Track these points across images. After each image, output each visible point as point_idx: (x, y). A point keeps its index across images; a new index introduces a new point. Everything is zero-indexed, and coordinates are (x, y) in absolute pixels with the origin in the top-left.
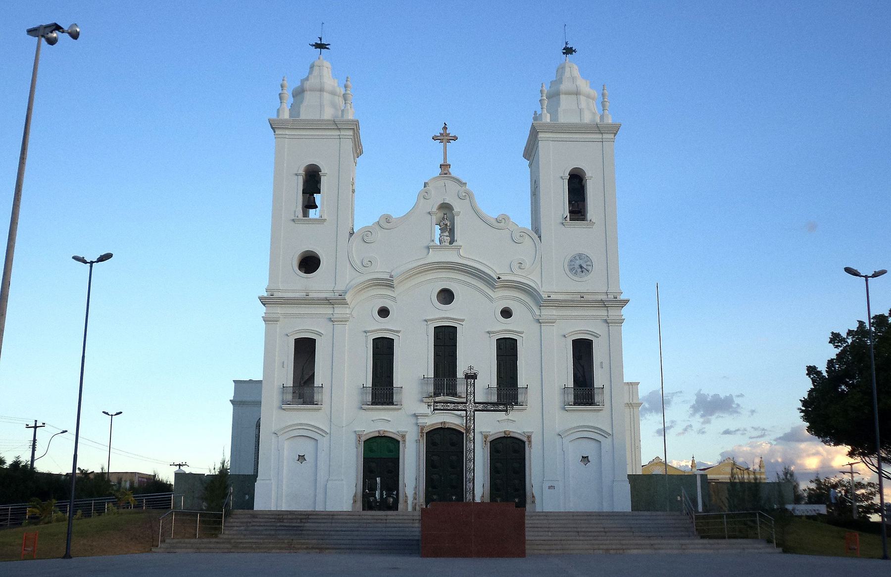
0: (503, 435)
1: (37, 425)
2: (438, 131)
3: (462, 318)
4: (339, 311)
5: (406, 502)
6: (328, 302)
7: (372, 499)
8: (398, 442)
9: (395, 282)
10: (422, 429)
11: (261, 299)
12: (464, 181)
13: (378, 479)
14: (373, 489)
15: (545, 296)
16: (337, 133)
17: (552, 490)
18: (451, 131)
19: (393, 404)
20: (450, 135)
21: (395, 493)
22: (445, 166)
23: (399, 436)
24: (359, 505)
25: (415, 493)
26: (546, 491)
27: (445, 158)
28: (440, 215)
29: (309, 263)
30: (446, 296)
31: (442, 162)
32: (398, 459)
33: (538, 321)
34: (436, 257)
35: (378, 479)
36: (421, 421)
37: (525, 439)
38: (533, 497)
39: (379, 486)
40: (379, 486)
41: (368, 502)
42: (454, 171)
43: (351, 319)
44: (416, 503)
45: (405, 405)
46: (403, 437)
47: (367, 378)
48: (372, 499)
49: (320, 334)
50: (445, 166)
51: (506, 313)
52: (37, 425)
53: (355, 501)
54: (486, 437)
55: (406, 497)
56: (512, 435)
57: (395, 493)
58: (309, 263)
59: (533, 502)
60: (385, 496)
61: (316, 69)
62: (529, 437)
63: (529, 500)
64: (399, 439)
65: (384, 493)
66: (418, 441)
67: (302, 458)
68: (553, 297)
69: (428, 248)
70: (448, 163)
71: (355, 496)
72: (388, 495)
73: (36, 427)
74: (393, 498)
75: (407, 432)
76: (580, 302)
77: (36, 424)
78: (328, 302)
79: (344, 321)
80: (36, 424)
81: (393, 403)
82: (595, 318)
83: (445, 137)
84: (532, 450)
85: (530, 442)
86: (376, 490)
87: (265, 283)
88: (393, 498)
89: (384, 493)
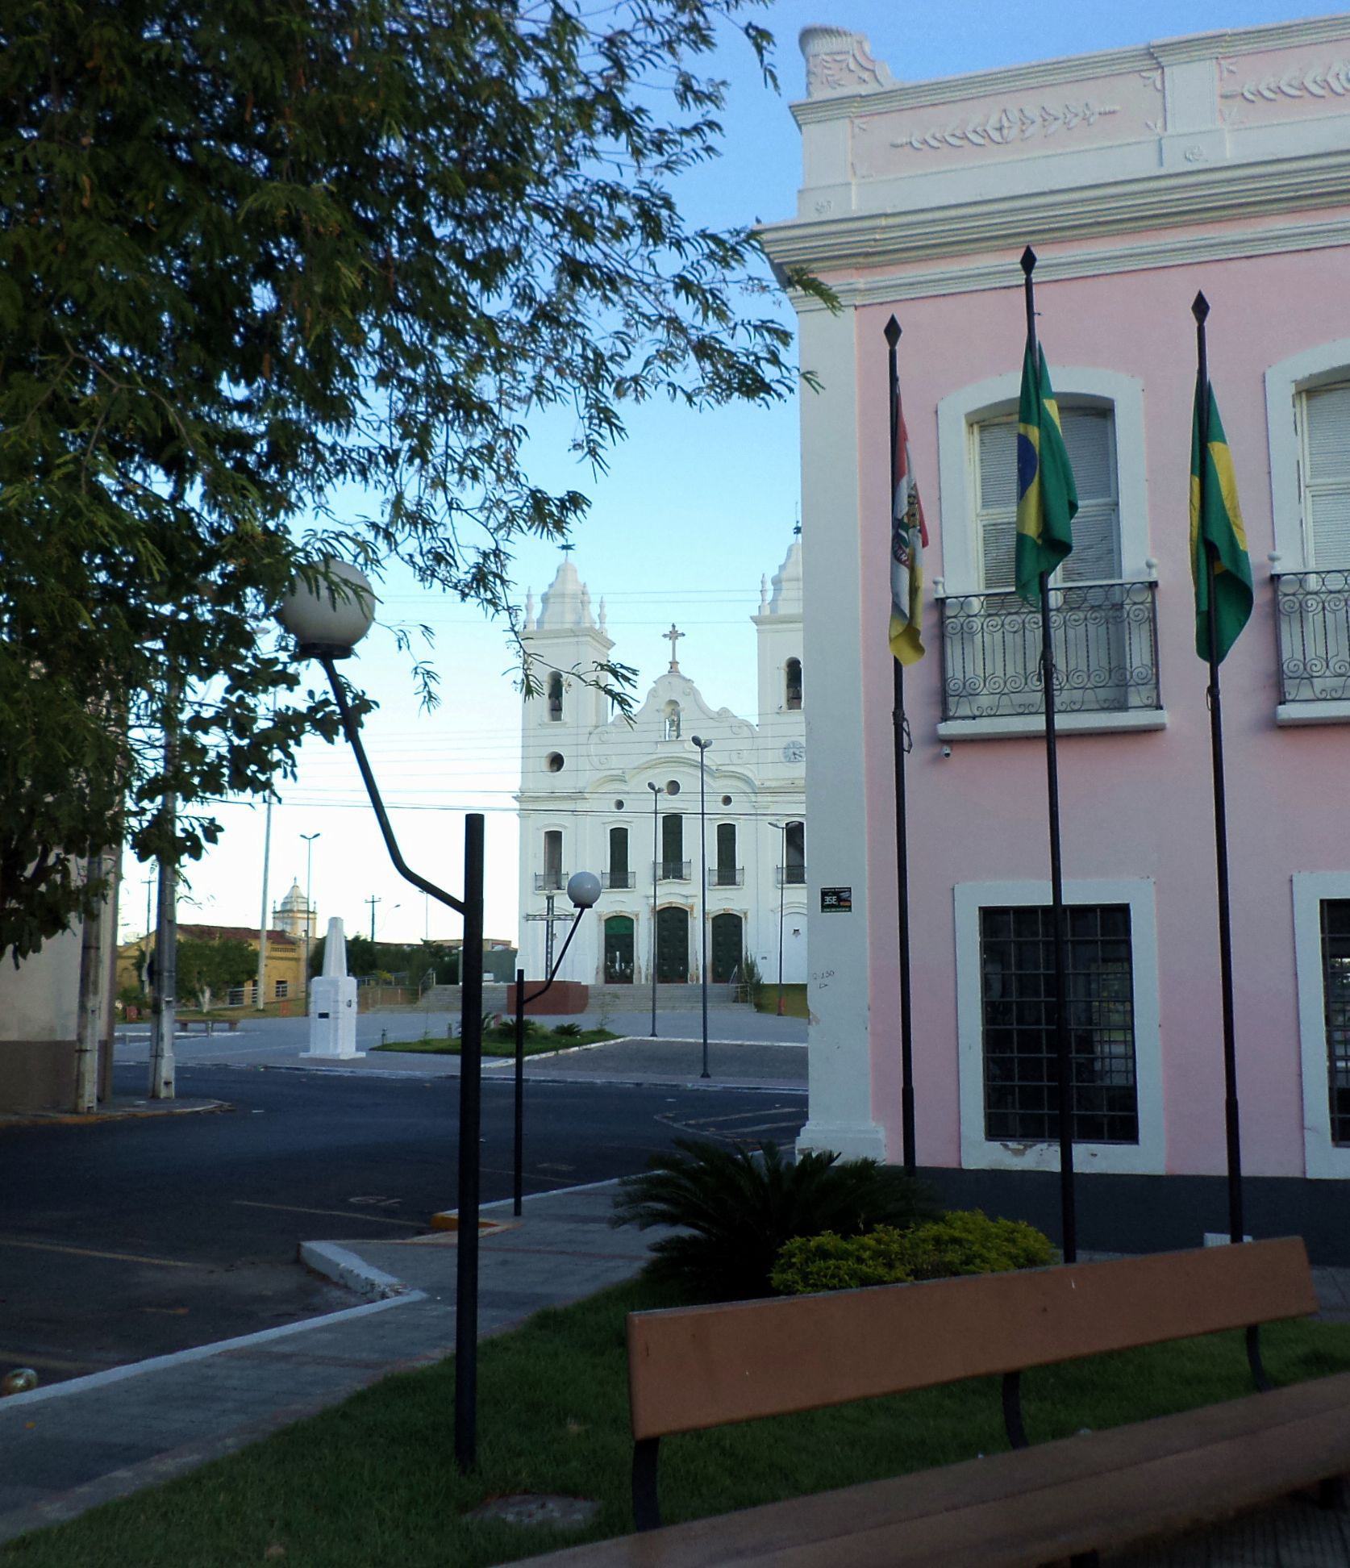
2: (668, 629)
5: (640, 972)
6: (570, 797)
9: (627, 778)
12: (688, 677)
14: (613, 961)
15: (757, 783)
16: (576, 639)
24: (602, 976)
28: (669, 710)
34: (664, 751)
41: (610, 976)
42: (680, 667)
46: (637, 915)
49: (565, 827)
58: (557, 761)
61: (561, 573)
64: (633, 917)
68: (767, 784)
69: (657, 742)
72: (626, 967)
78: (570, 797)
83: (674, 635)
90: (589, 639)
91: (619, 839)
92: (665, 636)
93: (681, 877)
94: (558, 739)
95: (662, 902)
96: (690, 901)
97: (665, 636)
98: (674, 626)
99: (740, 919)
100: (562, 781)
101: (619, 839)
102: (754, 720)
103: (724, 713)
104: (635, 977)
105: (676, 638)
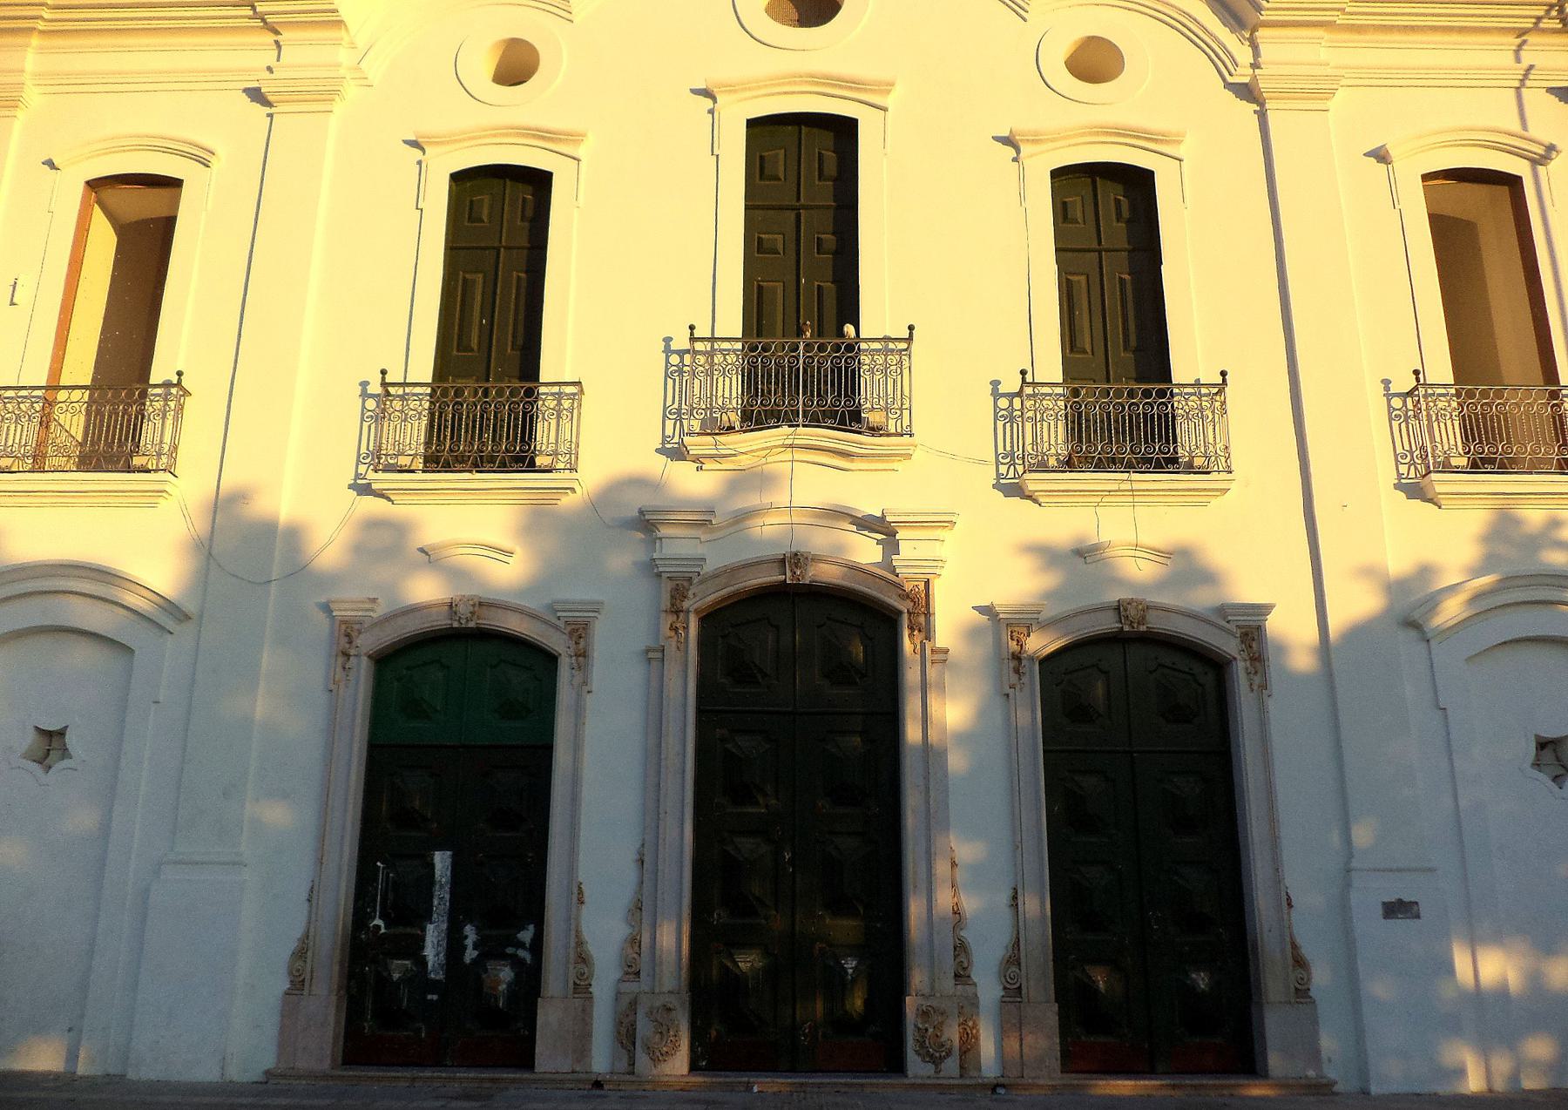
0: (1107, 624)
5: (581, 989)
7: (398, 968)
8: (551, 659)
10: (679, 594)
13: (441, 861)
17: (1399, 925)
19: (531, 467)
21: (526, 935)
23: (556, 627)
24: (324, 1004)
25: (634, 941)
26: (1371, 927)
32: (547, 750)
33: (1246, 92)
35: (441, 861)
39: (441, 898)
40: (441, 898)
43: (351, 90)
44: (633, 1004)
46: (579, 631)
48: (398, 968)
53: (298, 984)
55: (583, 959)
56: (1157, 623)
57: (526, 935)
59: (1302, 992)
60: (470, 954)
64: (556, 642)
65: (470, 933)
66: (654, 656)
67: (51, 743)
71: (301, 953)
72: (491, 950)
74: (517, 963)
75: (596, 608)
79: (324, 94)
81: (532, 463)
84: (1271, 705)
86: (427, 916)
88: (517, 963)
89: (470, 934)
93: (850, 419)
99: (1218, 666)
104: (550, 1016)
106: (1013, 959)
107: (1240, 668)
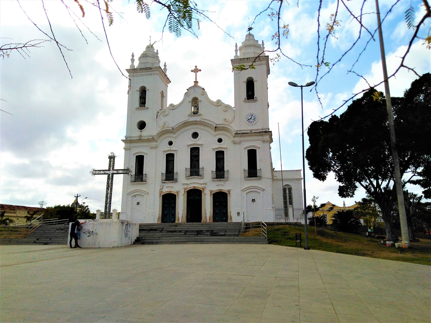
0: (218, 191)
1: (78, 196)
2: (193, 68)
3: (201, 143)
4: (153, 144)
5: (179, 220)
11: (123, 140)
18: (199, 68)
20: (198, 69)
22: (196, 82)
24: (160, 222)
25: (182, 216)
27: (196, 79)
29: (142, 125)
30: (195, 135)
31: (195, 81)
36: (185, 186)
37: (227, 193)
38: (231, 217)
45: (179, 180)
47: (163, 169)
50: (196, 82)
51: (220, 140)
52: (78, 196)
54: (211, 192)
55: (179, 218)
58: (142, 125)
62: (229, 192)
63: (229, 219)
67: (138, 203)
70: (197, 81)
73: (77, 197)
76: (251, 134)
77: (77, 195)
80: (77, 195)
82: (258, 140)
83: (196, 70)
85: (229, 194)
87: (125, 134)
90: (158, 72)
91: (170, 158)
92: (192, 71)
93: (198, 175)
94: (143, 115)
95: (191, 187)
96: (204, 186)
97: (192, 71)
98: (196, 67)
100: (146, 133)
101: (170, 158)
102: (232, 105)
103: (219, 103)
105: (197, 72)
106: (210, 217)
107: (228, 194)
